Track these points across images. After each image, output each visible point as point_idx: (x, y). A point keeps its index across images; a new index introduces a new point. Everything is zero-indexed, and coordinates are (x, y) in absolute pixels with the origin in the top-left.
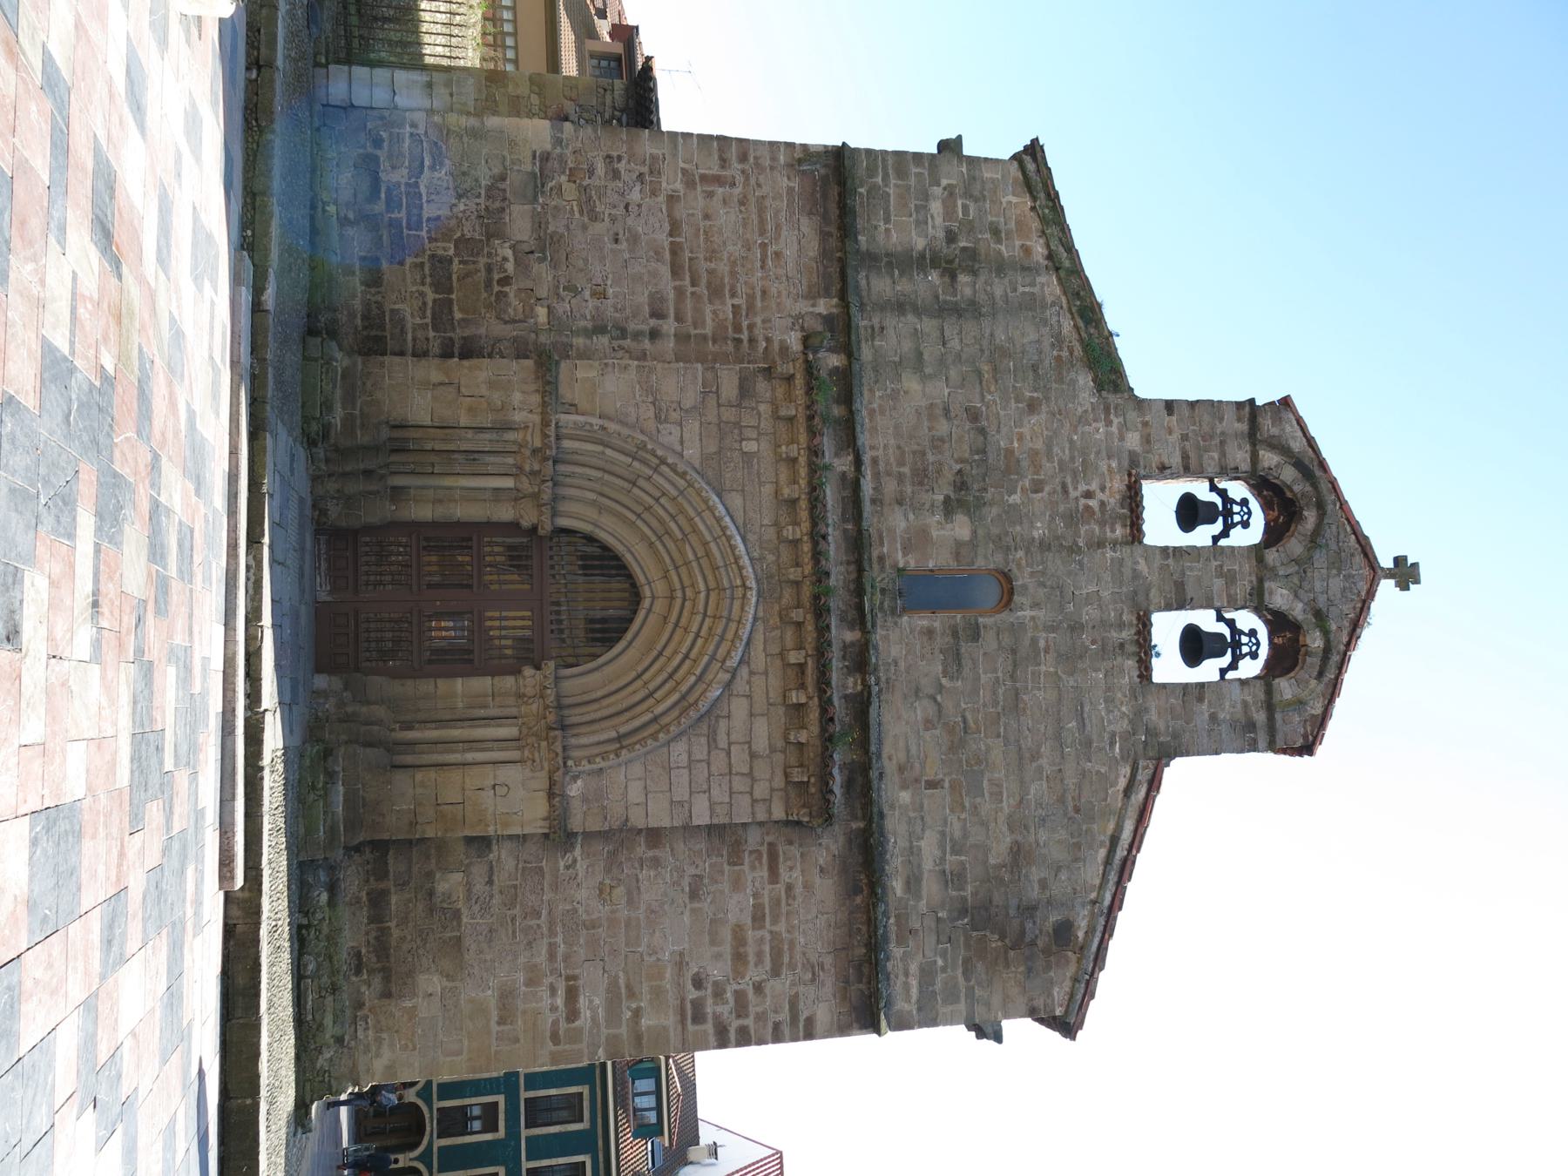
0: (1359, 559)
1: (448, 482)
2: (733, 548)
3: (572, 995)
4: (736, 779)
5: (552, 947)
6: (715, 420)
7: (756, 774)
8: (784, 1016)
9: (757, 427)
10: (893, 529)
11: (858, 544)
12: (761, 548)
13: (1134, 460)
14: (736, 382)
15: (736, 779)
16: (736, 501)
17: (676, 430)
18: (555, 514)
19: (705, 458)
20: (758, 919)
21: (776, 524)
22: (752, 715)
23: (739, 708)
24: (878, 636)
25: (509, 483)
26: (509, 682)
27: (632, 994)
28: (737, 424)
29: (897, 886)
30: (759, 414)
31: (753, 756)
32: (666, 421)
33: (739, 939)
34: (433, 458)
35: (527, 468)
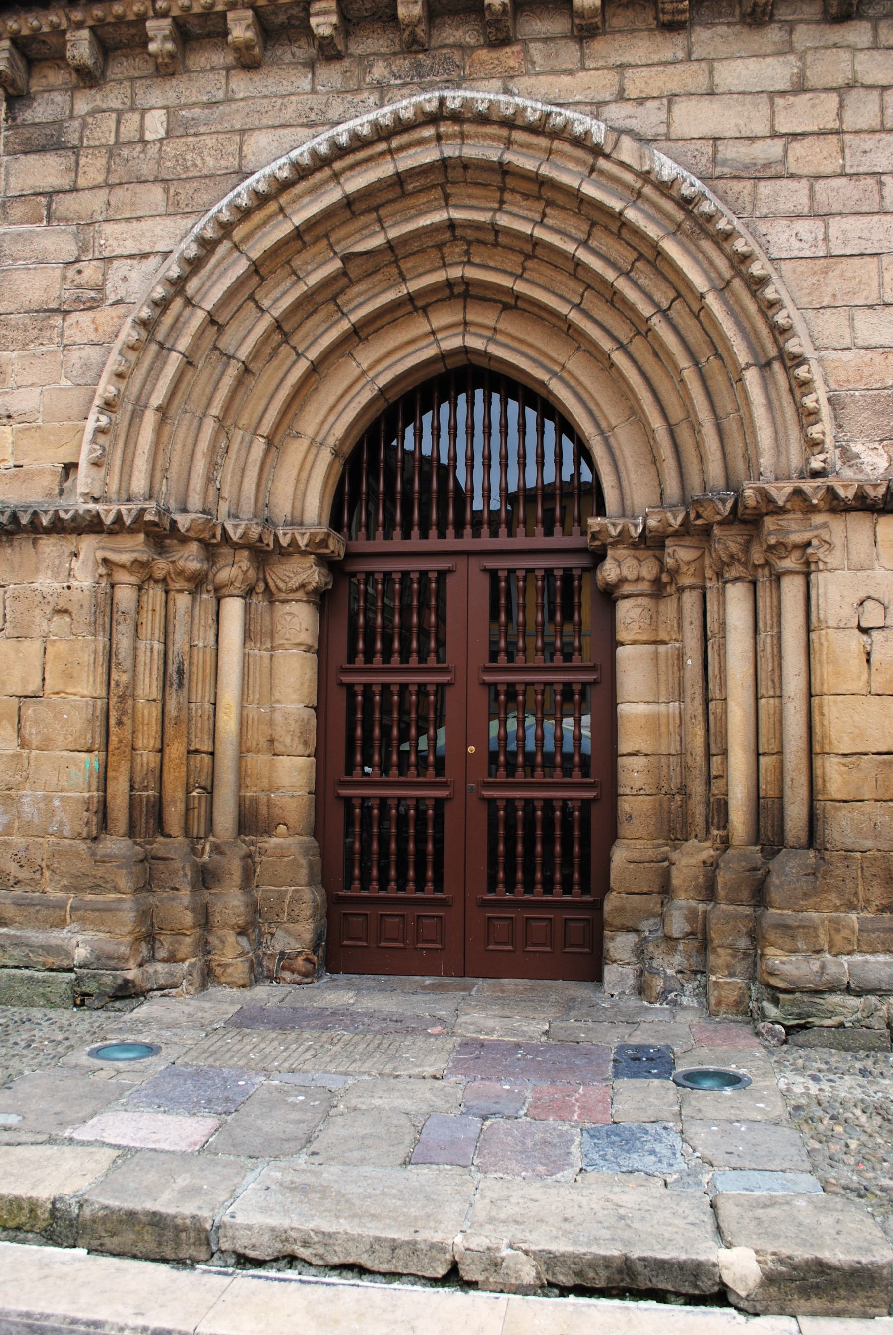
1: (228, 723)
2: (359, 142)
4: (852, 120)
6: (103, 194)
7: (840, 81)
9: (119, 113)
12: (359, 90)
14: (32, 158)
15: (852, 120)
16: (260, 143)
17: (120, 268)
18: (297, 522)
19: (174, 210)
21: (311, 65)
22: (712, 94)
23: (695, 118)
25: (233, 608)
26: (629, 613)
28: (112, 152)
30: (92, 113)
31: (800, 87)
32: (100, 289)
34: (176, 750)
35: (194, 566)
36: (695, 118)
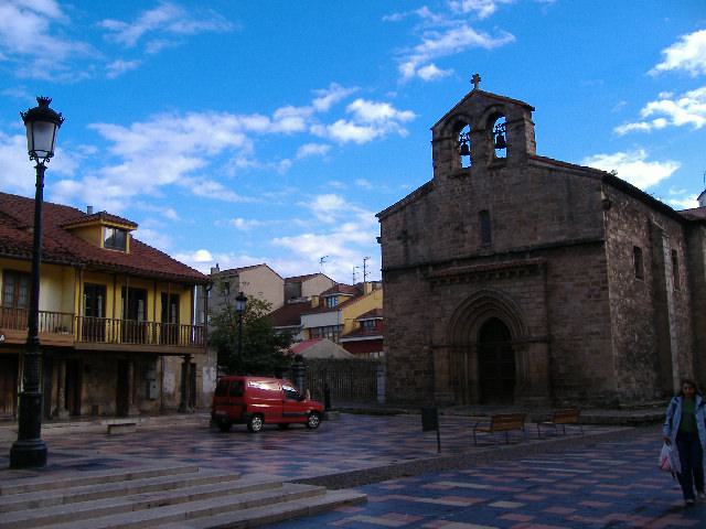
0: (472, 99)
3: (592, 334)
5: (580, 340)
8: (599, 270)
10: (468, 249)
11: (473, 258)
13: (448, 177)
20: (571, 280)
23: (513, 290)
24: (498, 251)
27: (592, 316)
29: (562, 238)
33: (577, 285)
36: (513, 290)
